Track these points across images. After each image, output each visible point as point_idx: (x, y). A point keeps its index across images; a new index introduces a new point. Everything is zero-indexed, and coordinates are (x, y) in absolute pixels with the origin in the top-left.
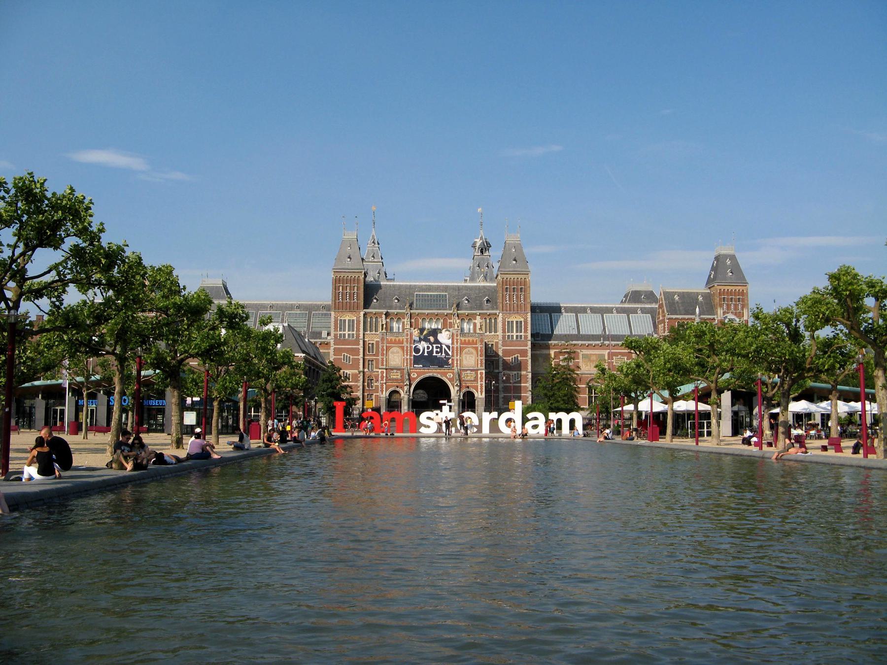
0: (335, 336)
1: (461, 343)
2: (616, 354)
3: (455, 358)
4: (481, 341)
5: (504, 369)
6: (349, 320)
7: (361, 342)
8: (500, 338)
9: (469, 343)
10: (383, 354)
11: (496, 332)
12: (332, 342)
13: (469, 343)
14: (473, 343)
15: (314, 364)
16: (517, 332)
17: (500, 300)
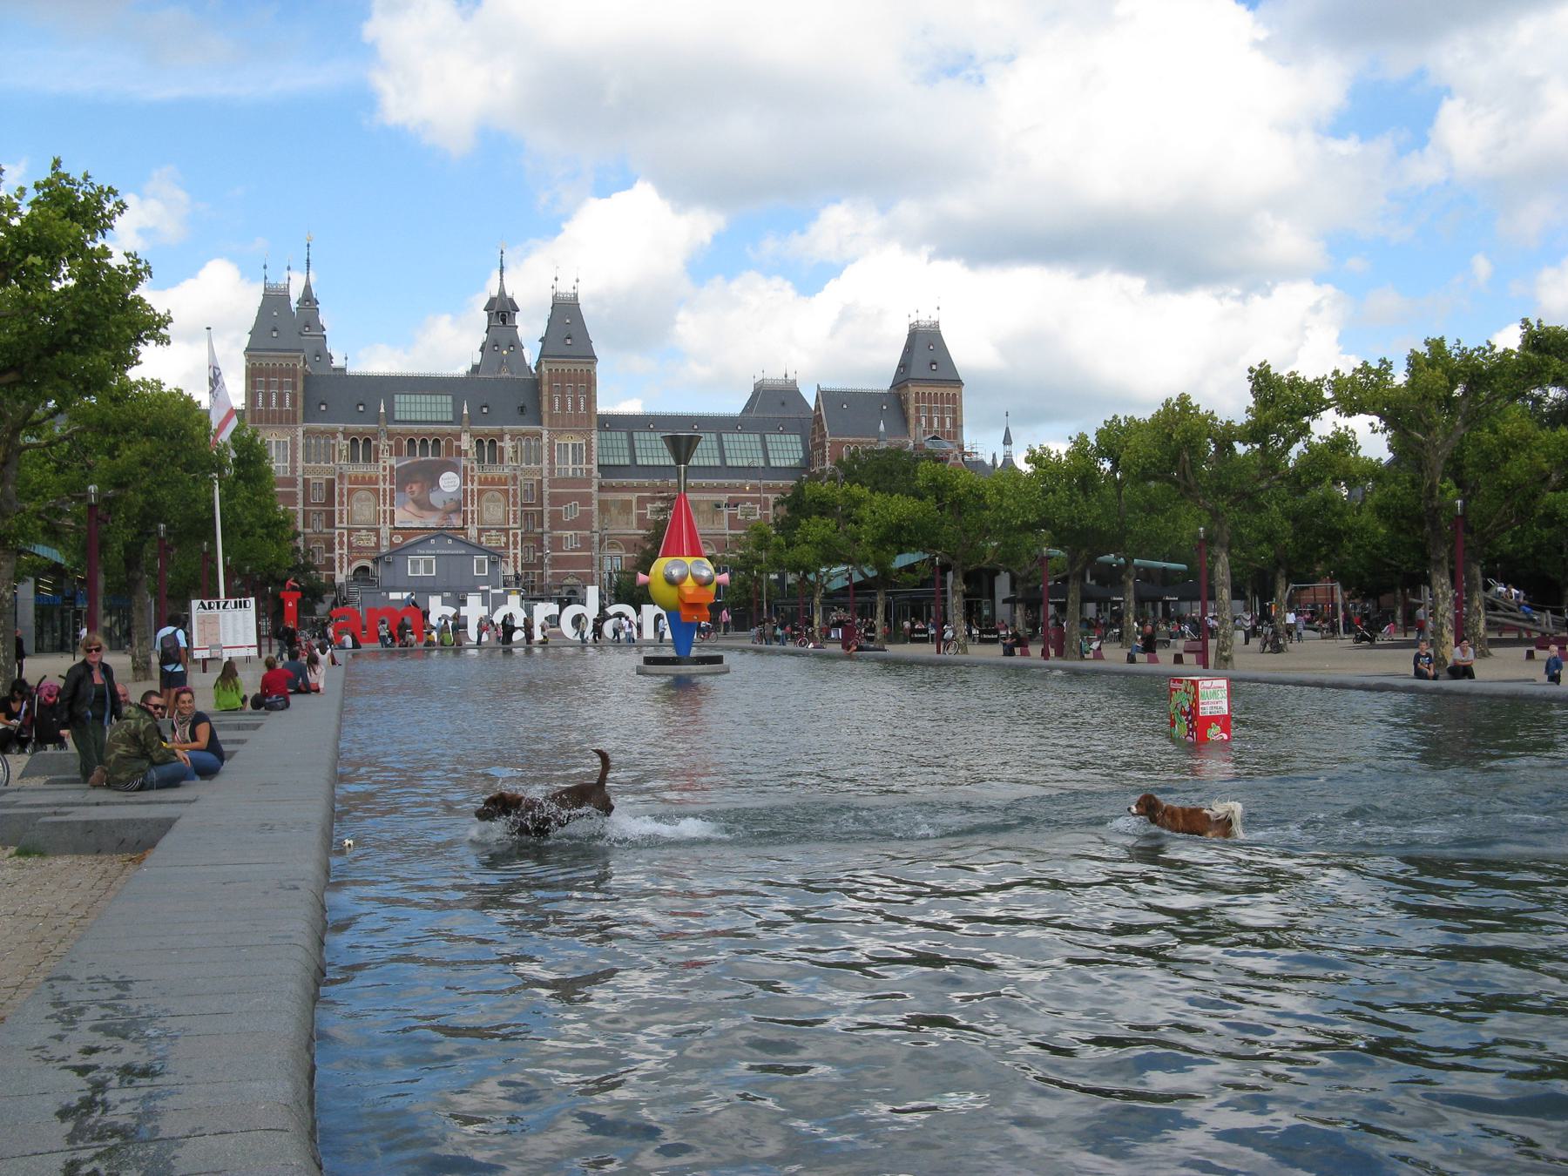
3: (470, 508)
5: (552, 528)
7: (300, 480)
8: (545, 473)
9: (493, 482)
10: (342, 503)
11: (539, 461)
13: (493, 482)
14: (502, 481)
17: (545, 407)
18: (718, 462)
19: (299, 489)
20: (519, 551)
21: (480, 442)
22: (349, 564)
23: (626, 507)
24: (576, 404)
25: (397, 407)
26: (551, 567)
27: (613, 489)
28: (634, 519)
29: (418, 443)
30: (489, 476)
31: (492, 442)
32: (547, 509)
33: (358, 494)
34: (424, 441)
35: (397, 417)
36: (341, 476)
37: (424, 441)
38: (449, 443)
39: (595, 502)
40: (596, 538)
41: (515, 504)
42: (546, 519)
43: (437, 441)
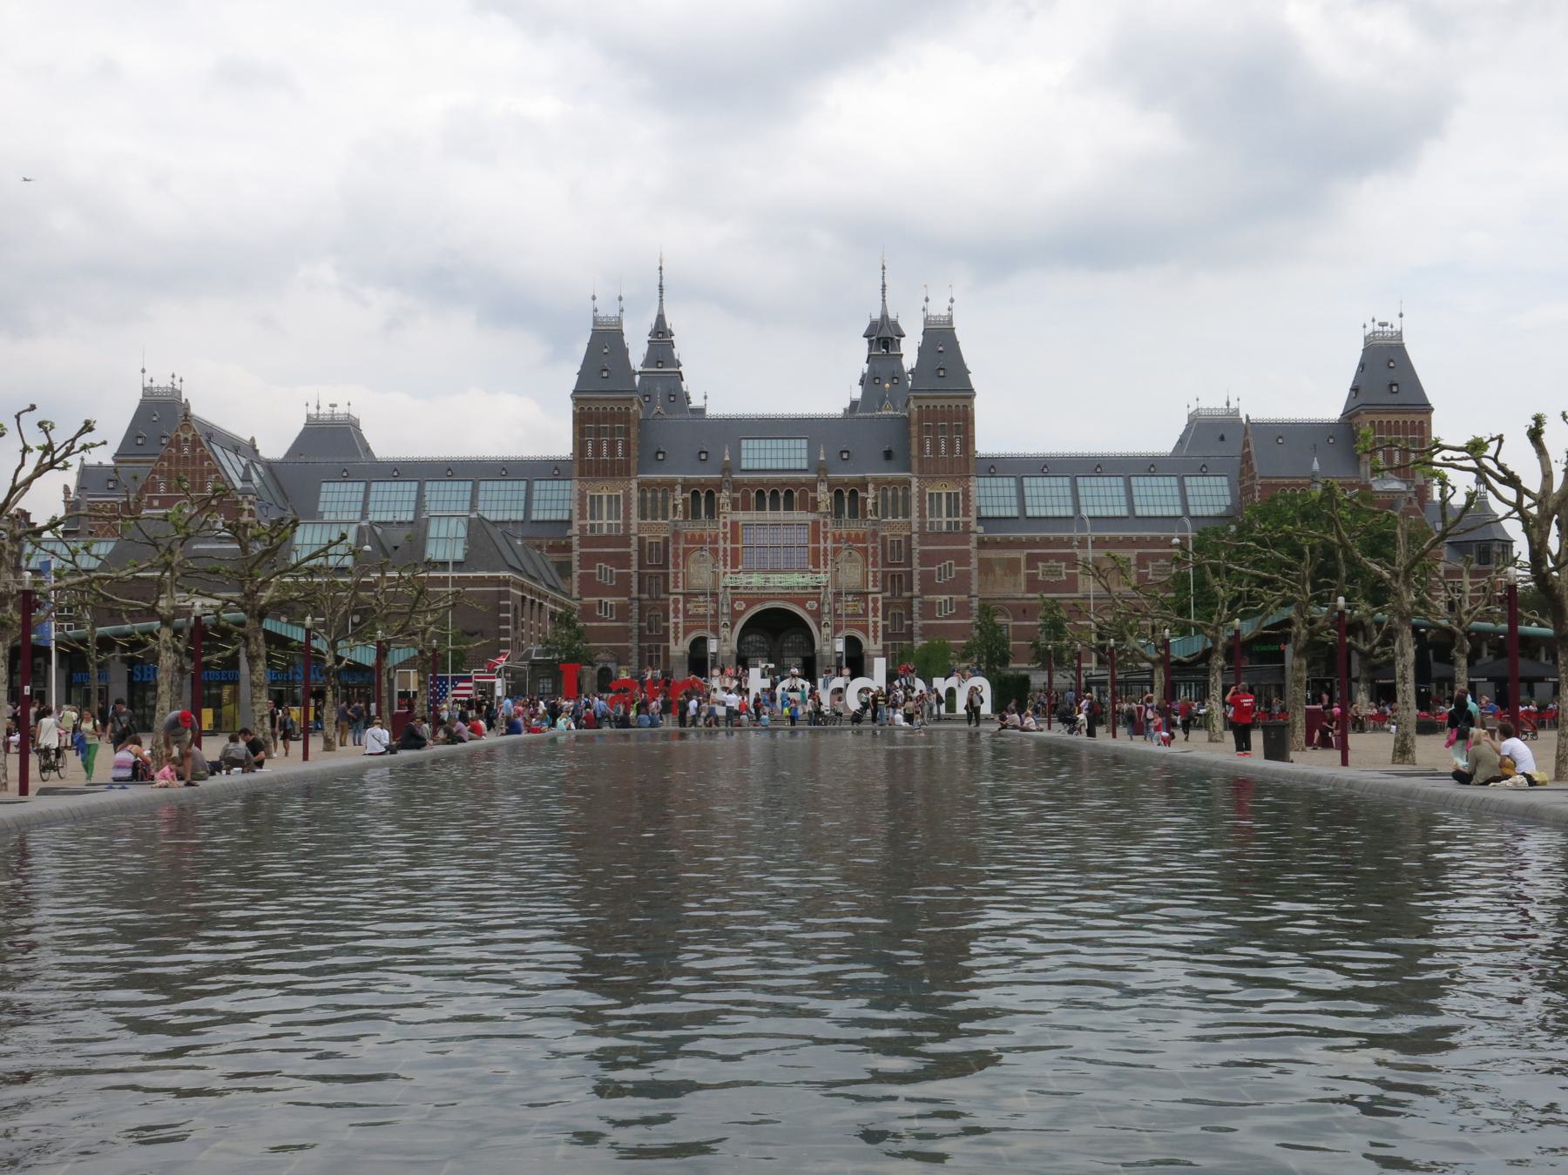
0: (583, 527)
1: (835, 541)
2: (1155, 557)
5: (924, 591)
6: (609, 497)
7: (634, 540)
8: (915, 528)
11: (907, 514)
12: (575, 541)
14: (858, 539)
15: (531, 591)
16: (949, 515)
17: (914, 452)
18: (1125, 512)
19: (633, 550)
20: (879, 619)
21: (839, 493)
22: (687, 631)
23: (1012, 566)
25: (744, 454)
26: (923, 636)
27: (997, 544)
28: (1022, 579)
29: (768, 494)
30: (844, 532)
31: (854, 493)
32: (917, 569)
34: (775, 493)
35: (744, 466)
36: (676, 534)
37: (775, 493)
38: (804, 494)
39: (974, 561)
40: (975, 603)
41: (875, 564)
42: (916, 582)
43: (789, 493)
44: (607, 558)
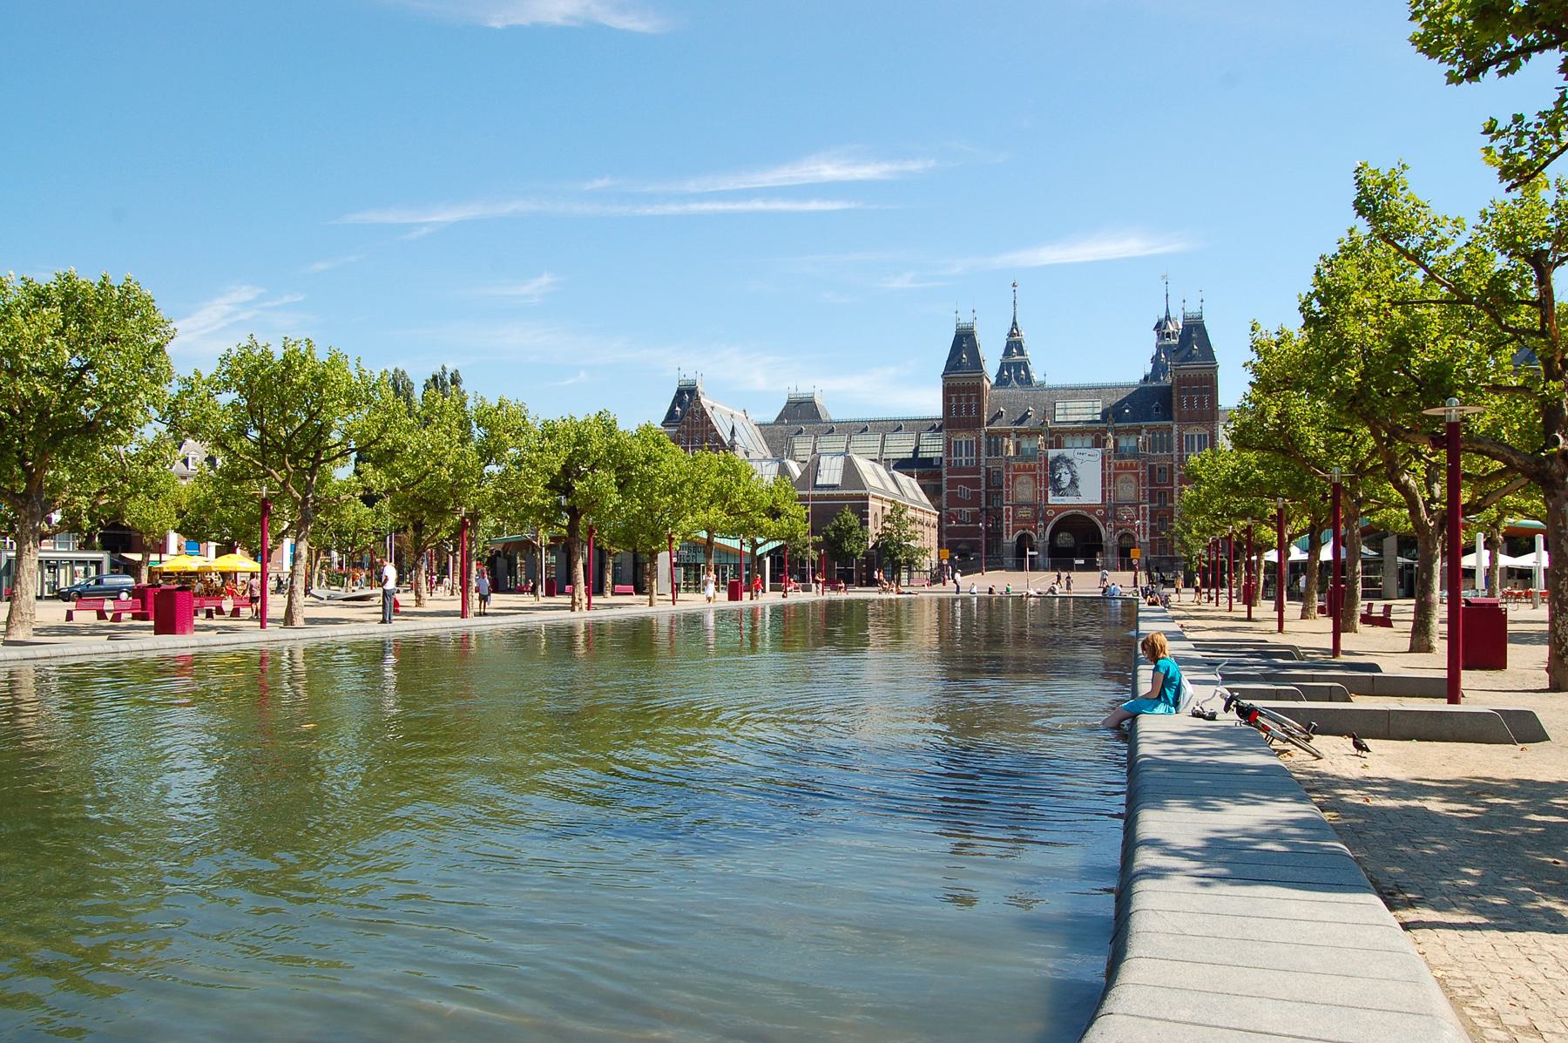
0: (949, 462)
4: (1144, 464)
7: (983, 470)
11: (1170, 449)
13: (1126, 468)
14: (1131, 467)
19: (982, 476)
24: (1201, 402)
33: (1019, 480)
44: (964, 482)
